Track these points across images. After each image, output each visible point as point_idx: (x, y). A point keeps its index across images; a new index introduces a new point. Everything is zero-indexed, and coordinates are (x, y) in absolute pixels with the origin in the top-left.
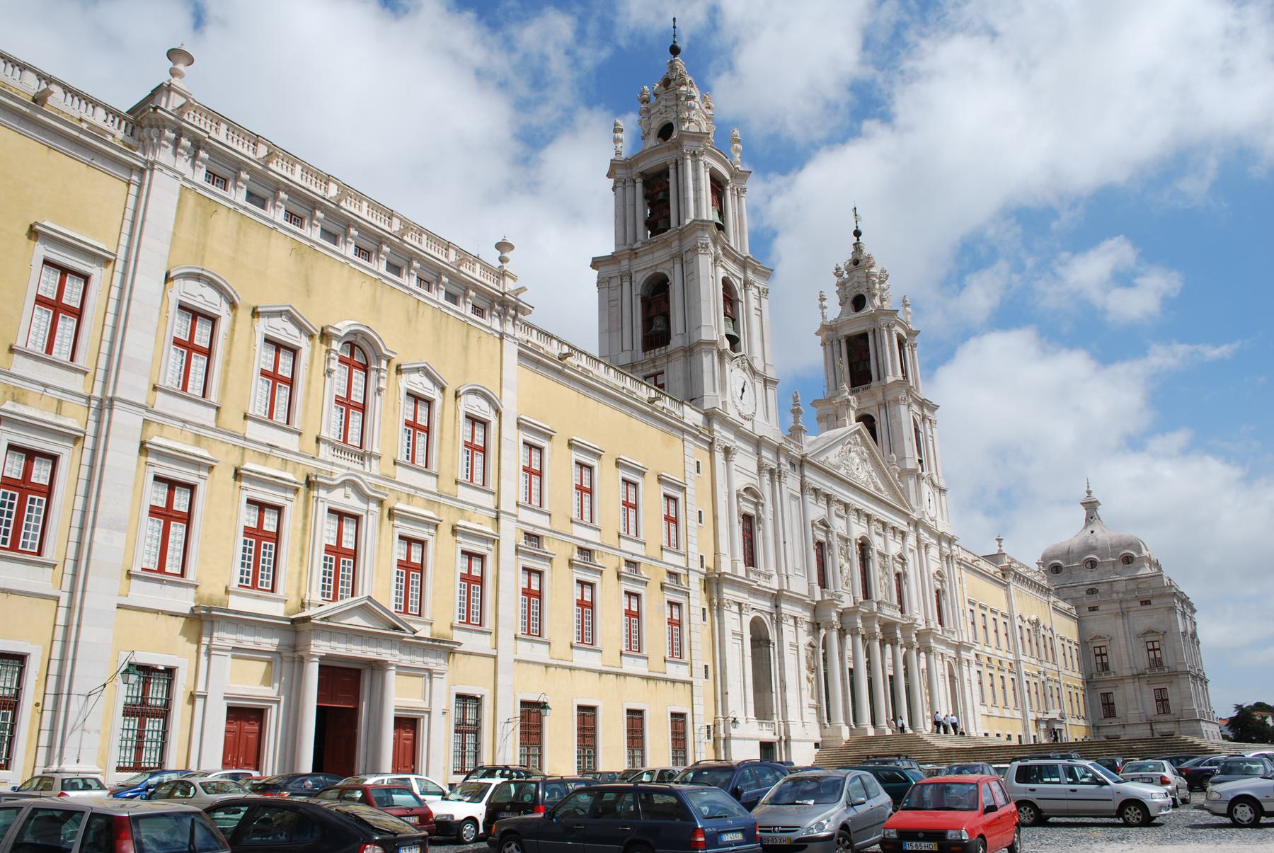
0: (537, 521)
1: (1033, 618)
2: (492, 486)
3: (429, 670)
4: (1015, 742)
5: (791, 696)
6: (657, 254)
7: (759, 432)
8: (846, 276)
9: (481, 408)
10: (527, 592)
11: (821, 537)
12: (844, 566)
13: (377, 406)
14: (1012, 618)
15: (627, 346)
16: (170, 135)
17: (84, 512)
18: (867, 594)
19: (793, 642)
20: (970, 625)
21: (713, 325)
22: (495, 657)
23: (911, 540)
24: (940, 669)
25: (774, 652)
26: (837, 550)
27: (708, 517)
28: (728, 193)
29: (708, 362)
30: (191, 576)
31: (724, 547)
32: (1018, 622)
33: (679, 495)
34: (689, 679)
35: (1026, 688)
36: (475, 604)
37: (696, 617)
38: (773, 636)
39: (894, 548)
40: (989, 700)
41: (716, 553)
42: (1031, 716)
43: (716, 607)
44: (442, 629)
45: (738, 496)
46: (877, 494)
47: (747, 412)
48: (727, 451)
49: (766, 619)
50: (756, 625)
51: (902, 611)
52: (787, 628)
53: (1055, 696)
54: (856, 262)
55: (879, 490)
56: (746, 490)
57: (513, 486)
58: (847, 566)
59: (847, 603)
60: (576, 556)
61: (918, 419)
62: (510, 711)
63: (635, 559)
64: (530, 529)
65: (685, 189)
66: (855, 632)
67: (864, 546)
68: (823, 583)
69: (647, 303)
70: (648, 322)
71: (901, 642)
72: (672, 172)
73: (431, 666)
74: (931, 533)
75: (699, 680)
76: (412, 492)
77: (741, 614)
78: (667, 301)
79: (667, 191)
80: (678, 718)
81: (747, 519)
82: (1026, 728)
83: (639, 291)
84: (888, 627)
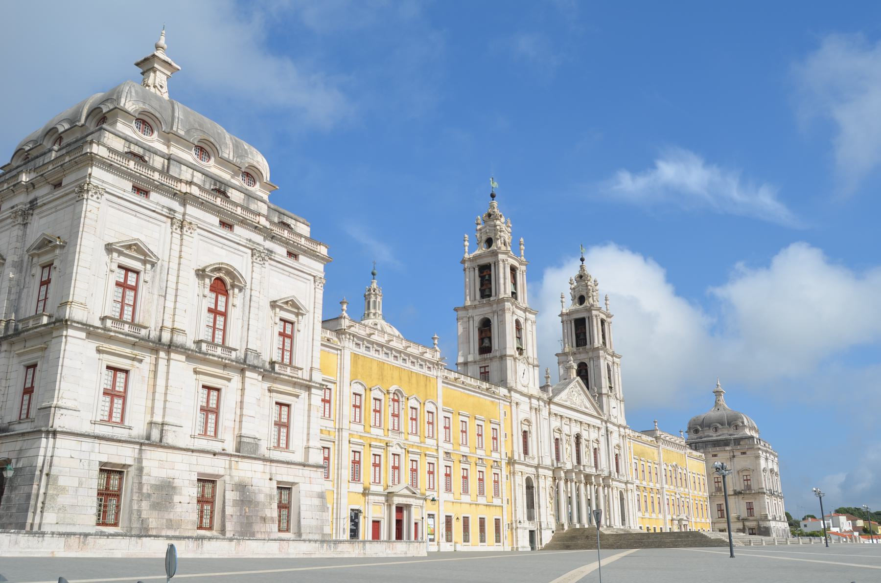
0: (448, 447)
1: (674, 464)
2: (435, 437)
4: (658, 531)
5: (543, 510)
7: (531, 392)
8: (575, 284)
9: (431, 407)
10: (446, 475)
11: (557, 436)
13: (402, 413)
14: (659, 464)
18: (579, 461)
19: (544, 486)
21: (511, 348)
23: (603, 431)
27: (509, 436)
29: (509, 362)
31: (515, 448)
32: (664, 467)
35: (666, 502)
38: (535, 485)
39: (594, 435)
41: (512, 452)
42: (669, 517)
44: (423, 491)
46: (586, 411)
47: (525, 384)
48: (517, 404)
49: (532, 477)
50: (528, 480)
51: (596, 466)
52: (542, 481)
54: (581, 277)
55: (586, 408)
58: (569, 448)
59: (569, 466)
61: (610, 364)
65: (499, 278)
66: (572, 481)
67: (578, 437)
68: (558, 459)
69: (481, 331)
70: (481, 340)
72: (493, 268)
74: (614, 424)
75: (505, 505)
79: (490, 275)
80: (497, 521)
82: (665, 524)
84: (588, 477)
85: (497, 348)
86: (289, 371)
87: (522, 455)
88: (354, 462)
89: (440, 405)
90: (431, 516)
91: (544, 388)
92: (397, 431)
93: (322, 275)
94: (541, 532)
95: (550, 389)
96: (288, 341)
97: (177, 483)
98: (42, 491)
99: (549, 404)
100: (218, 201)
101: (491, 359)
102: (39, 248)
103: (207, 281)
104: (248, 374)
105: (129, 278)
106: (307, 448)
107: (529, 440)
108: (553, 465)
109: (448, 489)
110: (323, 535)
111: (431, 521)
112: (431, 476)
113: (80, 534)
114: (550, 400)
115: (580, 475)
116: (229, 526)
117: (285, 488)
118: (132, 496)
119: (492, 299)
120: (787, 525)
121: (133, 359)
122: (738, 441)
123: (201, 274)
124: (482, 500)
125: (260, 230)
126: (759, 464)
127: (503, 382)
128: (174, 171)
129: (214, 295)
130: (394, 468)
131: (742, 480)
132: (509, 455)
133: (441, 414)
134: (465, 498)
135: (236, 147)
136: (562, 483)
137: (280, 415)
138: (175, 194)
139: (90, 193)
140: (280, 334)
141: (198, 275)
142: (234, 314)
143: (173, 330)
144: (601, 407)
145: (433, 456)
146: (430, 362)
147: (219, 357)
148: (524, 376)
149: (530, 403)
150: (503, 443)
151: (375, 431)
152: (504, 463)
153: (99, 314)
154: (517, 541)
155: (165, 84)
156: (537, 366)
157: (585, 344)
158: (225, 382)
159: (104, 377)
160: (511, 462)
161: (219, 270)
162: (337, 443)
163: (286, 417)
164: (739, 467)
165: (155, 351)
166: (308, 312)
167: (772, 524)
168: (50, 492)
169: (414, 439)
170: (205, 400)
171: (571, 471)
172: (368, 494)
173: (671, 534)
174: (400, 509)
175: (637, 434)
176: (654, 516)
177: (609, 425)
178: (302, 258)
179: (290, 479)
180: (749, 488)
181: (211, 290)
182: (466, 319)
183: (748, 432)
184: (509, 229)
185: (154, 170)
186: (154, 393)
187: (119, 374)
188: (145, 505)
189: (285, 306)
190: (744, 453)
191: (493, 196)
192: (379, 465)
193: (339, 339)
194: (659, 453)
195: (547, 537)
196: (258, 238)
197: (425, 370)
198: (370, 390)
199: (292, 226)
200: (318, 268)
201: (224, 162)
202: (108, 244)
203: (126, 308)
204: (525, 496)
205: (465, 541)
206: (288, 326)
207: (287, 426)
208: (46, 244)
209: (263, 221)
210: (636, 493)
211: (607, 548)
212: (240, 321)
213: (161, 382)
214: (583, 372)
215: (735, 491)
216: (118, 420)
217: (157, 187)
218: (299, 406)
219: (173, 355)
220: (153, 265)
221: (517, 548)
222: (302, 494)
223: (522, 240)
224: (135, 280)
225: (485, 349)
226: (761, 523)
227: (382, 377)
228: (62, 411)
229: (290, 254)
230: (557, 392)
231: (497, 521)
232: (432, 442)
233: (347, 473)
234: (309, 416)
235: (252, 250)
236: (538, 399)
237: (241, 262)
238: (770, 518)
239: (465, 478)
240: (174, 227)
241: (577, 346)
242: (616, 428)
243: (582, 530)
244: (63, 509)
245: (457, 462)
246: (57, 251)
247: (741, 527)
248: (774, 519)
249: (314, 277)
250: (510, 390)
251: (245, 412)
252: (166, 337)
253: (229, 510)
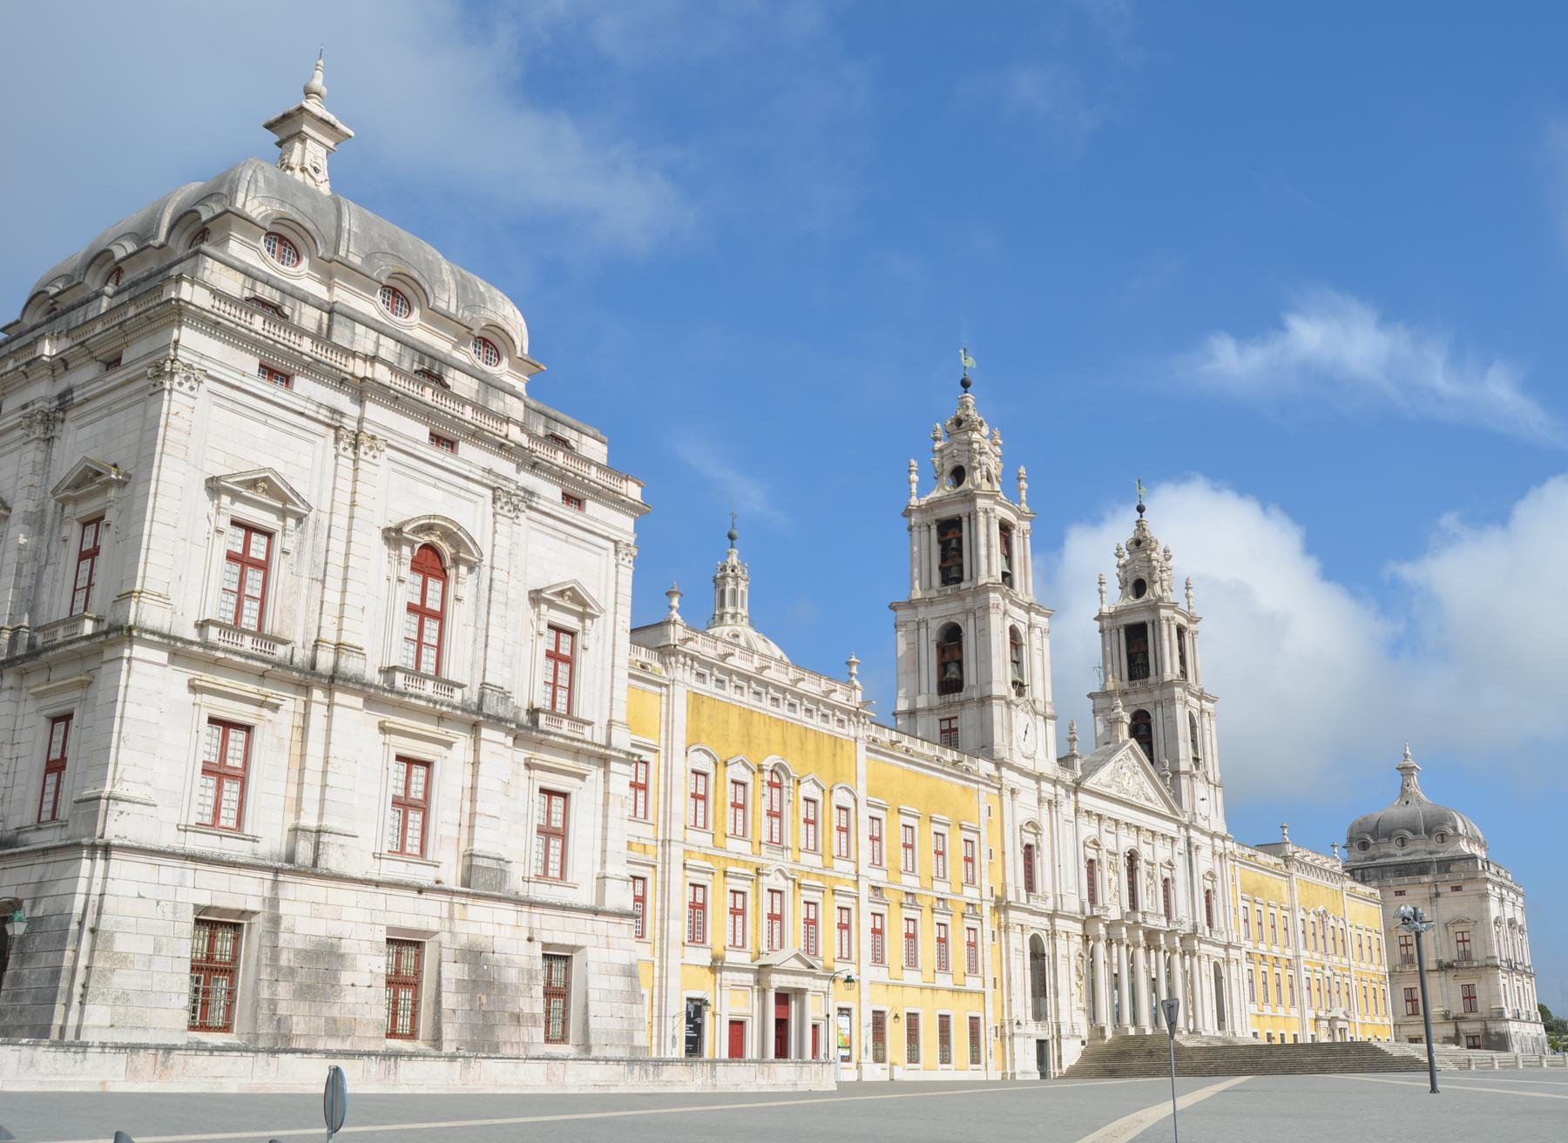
0: (878, 876)
1: (1321, 909)
2: (853, 857)
4: (1289, 1040)
5: (1063, 1000)
6: (951, 605)
7: (1039, 769)
8: (1127, 557)
10: (874, 931)
11: (1092, 854)
12: (1113, 883)
13: (788, 811)
14: (1291, 910)
15: (924, 689)
16: (682, 660)
17: (662, 910)
20: (1242, 923)
21: (1001, 683)
23: (1181, 845)
24: (1207, 969)
25: (1048, 962)
26: (1105, 865)
28: (1015, 537)
29: (998, 710)
30: (708, 943)
31: (1010, 880)
32: (1300, 915)
35: (1305, 985)
36: (845, 942)
37: (988, 939)
38: (1048, 951)
39: (1163, 852)
40: (1260, 996)
41: (1004, 886)
42: (1310, 1014)
44: (829, 962)
45: (1021, 829)
46: (1149, 805)
48: (1013, 791)
49: (1043, 935)
50: (1035, 942)
52: (1061, 942)
53: (1343, 994)
54: (1138, 542)
57: (865, 855)
58: (1115, 878)
59: (1114, 914)
61: (1196, 713)
62: (868, 1019)
65: (977, 545)
66: (1120, 942)
67: (1132, 857)
68: (1093, 899)
69: (942, 650)
70: (943, 667)
71: (1164, 947)
74: (1203, 832)
75: (989, 990)
78: (960, 648)
79: (960, 540)
80: (974, 1023)
82: (1303, 1027)
84: (1151, 935)
85: (973, 682)
86: (566, 727)
87: (1023, 892)
88: (694, 906)
89: (862, 794)
90: (843, 1011)
91: (1065, 761)
92: (778, 845)
93: (631, 540)
94: (1059, 1044)
95: (1078, 762)
96: (563, 668)
97: (346, 947)
98: (83, 962)
99: (1075, 793)
100: (428, 395)
101: (962, 704)
102: (77, 485)
103: (406, 551)
104: (485, 733)
105: (253, 546)
106: (602, 879)
107: (1037, 862)
108: (1083, 913)
109: (878, 958)
110: (634, 1048)
111: (844, 1022)
112: (845, 933)
113: (157, 1047)
114: (1078, 784)
115: (1138, 933)
116: (449, 1032)
117: (558, 957)
118: (258, 973)
119: (963, 585)
120: (1541, 1029)
121: (262, 704)
122: (1445, 865)
123: (393, 536)
124: (944, 981)
125: (509, 450)
126: (1487, 910)
127: (985, 749)
128: (340, 336)
129: (418, 579)
130: (772, 917)
131: (1453, 941)
132: (998, 892)
133: (865, 813)
134: (912, 977)
135: (463, 288)
136: (1101, 947)
137: (549, 813)
138: (343, 381)
139: (177, 379)
140: (549, 655)
141: (387, 539)
142: (459, 616)
143: (339, 647)
144: (1178, 798)
145: (847, 895)
146: (842, 710)
147: (429, 700)
148: (1027, 738)
149: (1039, 789)
151: (735, 846)
152: (986, 909)
153: (194, 616)
154: (1013, 1060)
155: (323, 164)
156: (1053, 718)
157: (1147, 675)
158: (441, 749)
159: (204, 738)
160: (1001, 906)
161: (428, 528)
162: (659, 868)
163: (560, 817)
164: (1447, 917)
165: (304, 688)
166: (603, 611)
167: (1513, 1027)
168: (99, 964)
169: (814, 861)
170: (401, 785)
171: (1119, 923)
172: (722, 969)
173: (1315, 1046)
174: (783, 998)
175: (1248, 851)
176: (1281, 1011)
177: (1192, 833)
178: (591, 506)
179: (569, 939)
180: (1467, 956)
181: (413, 569)
182: (912, 626)
183: (1465, 848)
184: (998, 450)
185: (302, 332)
186: (302, 770)
187: (233, 734)
188: (283, 989)
189: (558, 601)
190: (1457, 889)
191: (965, 384)
192: (742, 912)
193: (664, 664)
194: (1291, 889)
195: (1071, 1053)
196: (506, 467)
197: (833, 726)
198: (726, 764)
199: (573, 443)
200: (623, 525)
201: (439, 318)
202: (212, 479)
203: (247, 603)
204: (1028, 973)
205: (910, 1061)
206: (565, 640)
207: (562, 835)
208: (89, 478)
209: (515, 434)
210: (1246, 966)
211: (1189, 1075)
212: (471, 630)
213: (315, 749)
214: (1142, 728)
215: (1439, 962)
216: (232, 824)
217: (307, 366)
218: (586, 795)
219: (339, 697)
220: (300, 519)
221: (1013, 1075)
222: (592, 968)
223: (1022, 470)
224: (264, 549)
225: (950, 684)
226: (1490, 1025)
227: (748, 739)
228: (122, 806)
229: (567, 498)
230: (1091, 769)
231: (974, 1023)
232: (848, 867)
233: (679, 927)
234: (605, 816)
235: (494, 489)
236: (1055, 782)
237: (471, 514)
238: (1508, 1015)
239: (911, 937)
240: (342, 445)
241: (1131, 678)
242: (1207, 840)
243: (1141, 1038)
244: (123, 997)
246: (113, 493)
247: (1452, 1033)
248: (1517, 1018)
249: (616, 542)
250: (999, 764)
251: (480, 807)
252: (325, 661)
253: (449, 1000)
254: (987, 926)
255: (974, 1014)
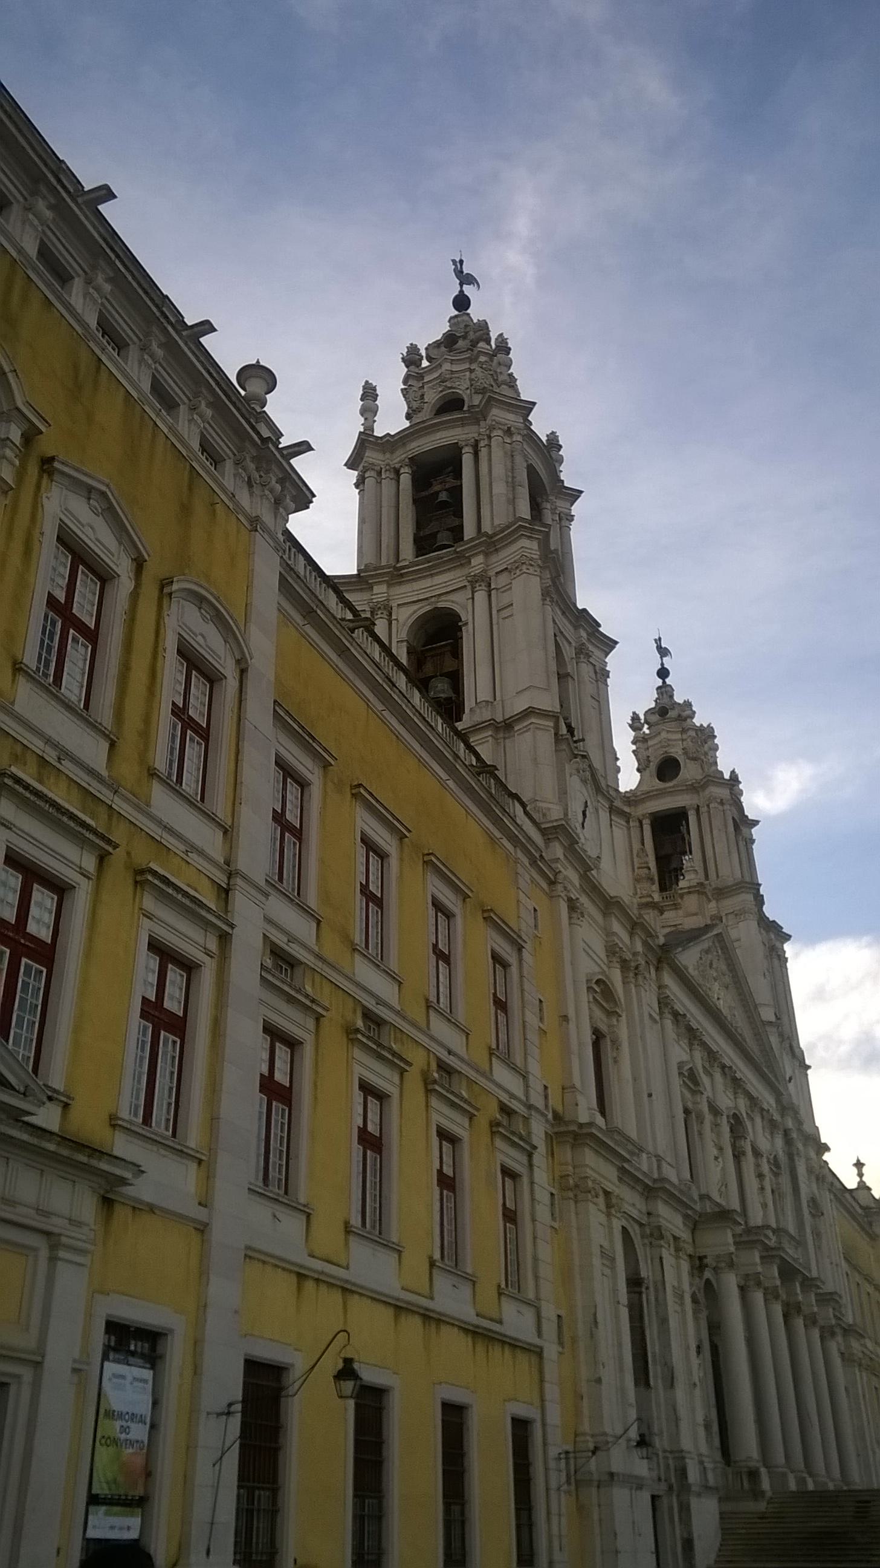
3: (48, 1234)
22: (202, 1229)
33: (511, 958)
34: (536, 1341)
36: (163, 1082)
37: (543, 1212)
43: (572, 1189)
44: (89, 1122)
56: (598, 982)
60: (360, 1023)
62: (227, 1383)
63: (451, 1061)
64: (280, 940)
72: (467, 460)
73: (56, 1224)
75: (551, 1351)
76: (51, 755)
77: (609, 1215)
78: (456, 652)
79: (457, 492)
81: (598, 1037)
83: (404, 635)
90: (134, 1341)
109: (277, 1180)
111: (127, 1386)
132: (555, 1101)
134: (369, 1266)
145: (189, 907)
150: (533, 1036)
152: (538, 1130)
239: (372, 1142)
245: (332, 1033)
254: (541, 1176)
255: (522, 1411)
